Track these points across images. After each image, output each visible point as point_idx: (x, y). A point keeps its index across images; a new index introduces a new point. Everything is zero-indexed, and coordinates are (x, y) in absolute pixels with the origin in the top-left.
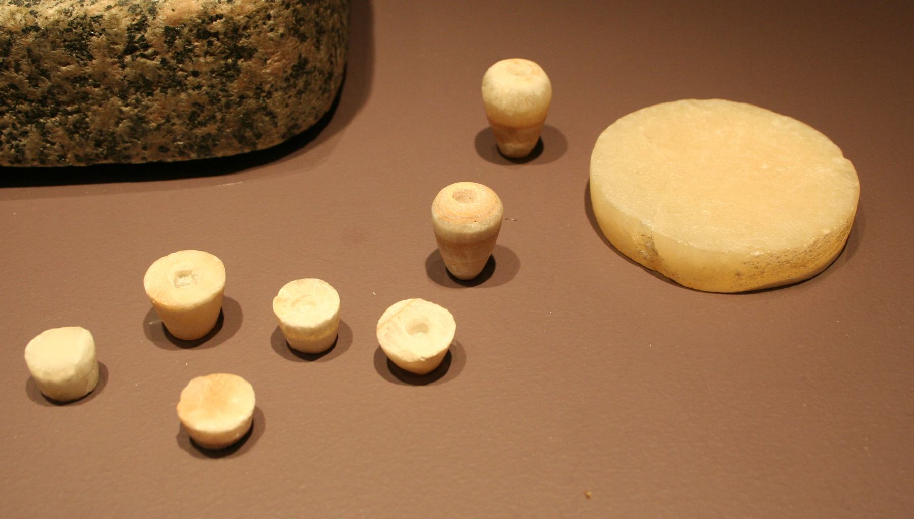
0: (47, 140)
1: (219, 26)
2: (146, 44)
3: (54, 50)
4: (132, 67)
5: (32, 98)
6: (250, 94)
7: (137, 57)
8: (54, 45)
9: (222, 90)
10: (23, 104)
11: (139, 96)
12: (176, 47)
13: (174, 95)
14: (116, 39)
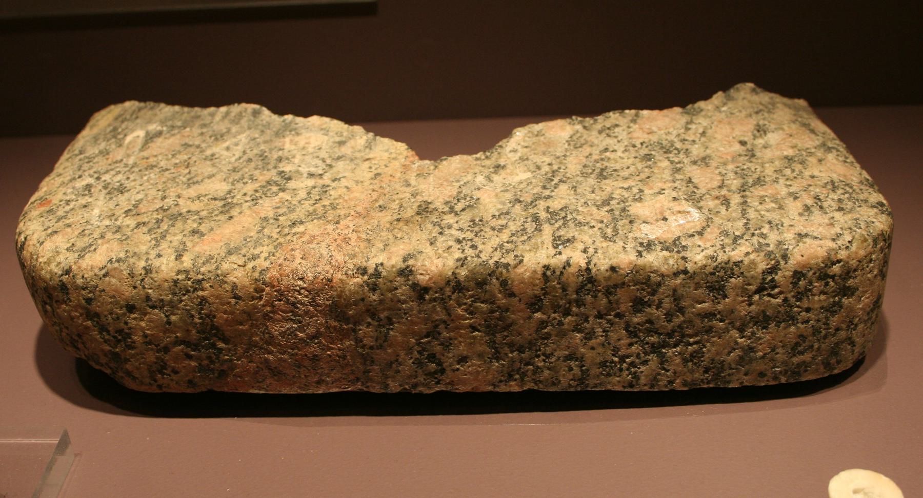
0: (663, 367)
1: (837, 270)
2: (775, 285)
3: (696, 290)
4: (758, 305)
5: (661, 331)
6: (844, 326)
7: (764, 295)
8: (697, 286)
9: (824, 324)
10: (652, 336)
11: (755, 329)
12: (799, 287)
13: (785, 328)
14: (752, 281)
